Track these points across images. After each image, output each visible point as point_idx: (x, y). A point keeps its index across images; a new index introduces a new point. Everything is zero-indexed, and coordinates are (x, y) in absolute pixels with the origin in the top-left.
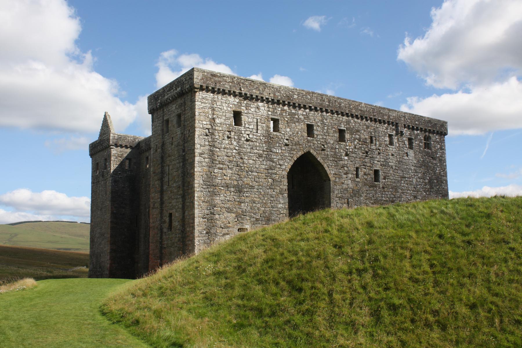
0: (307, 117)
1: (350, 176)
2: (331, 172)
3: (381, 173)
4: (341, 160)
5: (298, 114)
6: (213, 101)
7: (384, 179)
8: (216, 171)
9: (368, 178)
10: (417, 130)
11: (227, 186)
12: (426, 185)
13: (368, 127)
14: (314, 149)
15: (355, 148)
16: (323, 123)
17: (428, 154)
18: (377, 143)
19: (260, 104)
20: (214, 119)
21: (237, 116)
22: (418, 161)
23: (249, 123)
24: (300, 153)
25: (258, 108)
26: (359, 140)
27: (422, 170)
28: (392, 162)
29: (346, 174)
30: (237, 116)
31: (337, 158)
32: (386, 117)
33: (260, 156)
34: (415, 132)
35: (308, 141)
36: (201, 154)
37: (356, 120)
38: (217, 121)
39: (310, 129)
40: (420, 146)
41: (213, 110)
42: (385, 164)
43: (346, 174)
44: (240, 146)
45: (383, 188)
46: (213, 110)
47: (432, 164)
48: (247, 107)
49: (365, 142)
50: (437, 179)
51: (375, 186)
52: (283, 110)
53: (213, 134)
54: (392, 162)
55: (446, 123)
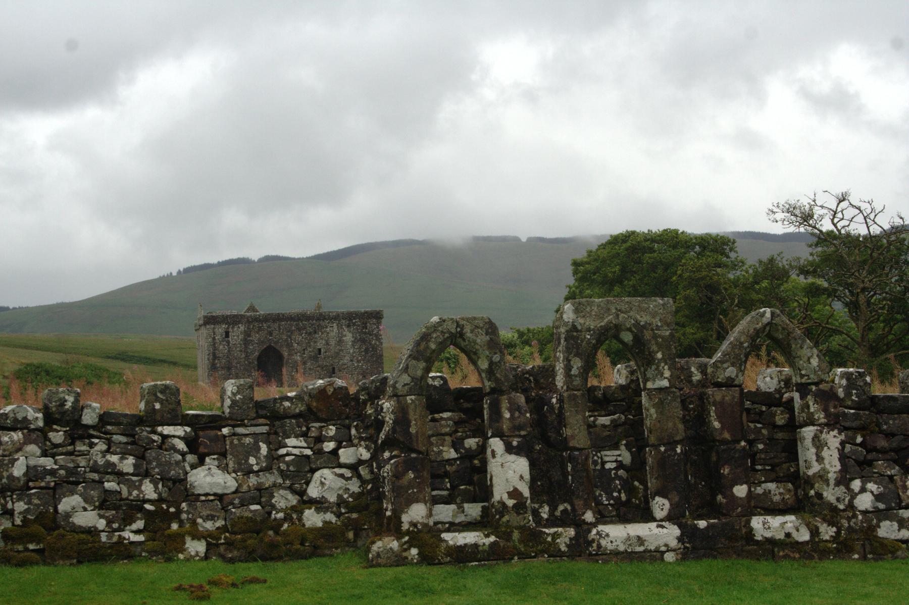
0: (269, 327)
1: (299, 354)
2: (286, 354)
3: (322, 350)
4: (292, 346)
5: (263, 326)
6: (214, 328)
7: (326, 352)
8: (216, 361)
9: (312, 354)
10: (355, 319)
11: (222, 368)
12: (362, 352)
13: (312, 325)
14: (274, 343)
15: (303, 338)
16: (280, 329)
17: (365, 333)
18: (320, 333)
19: (240, 325)
20: (214, 337)
21: (227, 334)
22: (356, 339)
23: (234, 336)
24: (265, 346)
25: (239, 327)
26: (306, 333)
27: (359, 343)
28: (333, 342)
29: (296, 353)
30: (227, 334)
31: (289, 346)
32: (327, 317)
33: (241, 351)
34: (354, 321)
35: (270, 339)
36: (208, 355)
37: (304, 322)
38: (216, 338)
39: (271, 334)
40: (358, 329)
41: (214, 333)
42: (327, 344)
43: (296, 353)
44: (229, 348)
45: (325, 358)
46: (214, 333)
47: (369, 338)
48: (233, 328)
49: (310, 334)
50: (373, 348)
51: (318, 358)
52: (254, 326)
53: (214, 344)
54: (333, 342)
55: (382, 311)
